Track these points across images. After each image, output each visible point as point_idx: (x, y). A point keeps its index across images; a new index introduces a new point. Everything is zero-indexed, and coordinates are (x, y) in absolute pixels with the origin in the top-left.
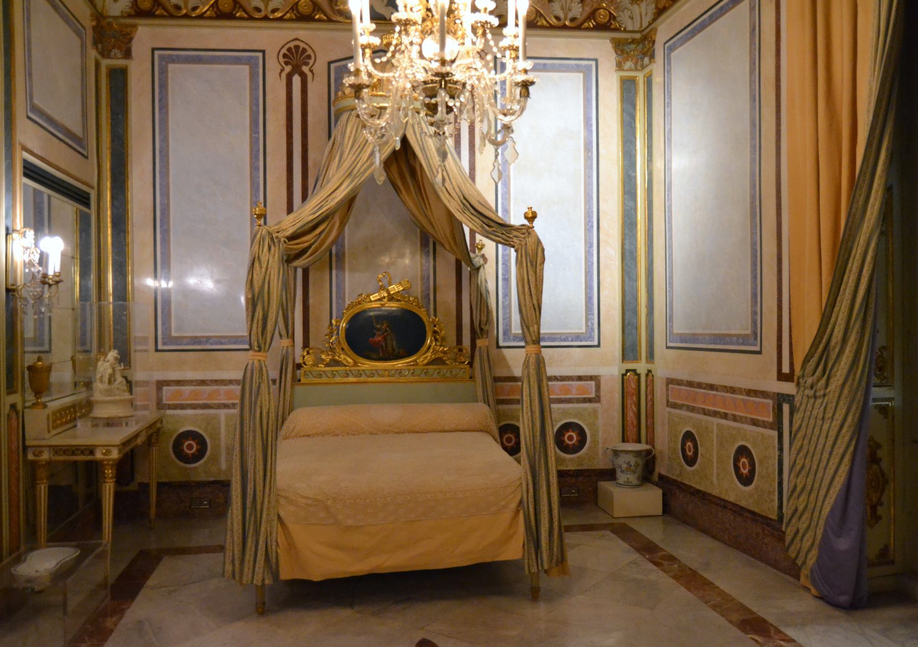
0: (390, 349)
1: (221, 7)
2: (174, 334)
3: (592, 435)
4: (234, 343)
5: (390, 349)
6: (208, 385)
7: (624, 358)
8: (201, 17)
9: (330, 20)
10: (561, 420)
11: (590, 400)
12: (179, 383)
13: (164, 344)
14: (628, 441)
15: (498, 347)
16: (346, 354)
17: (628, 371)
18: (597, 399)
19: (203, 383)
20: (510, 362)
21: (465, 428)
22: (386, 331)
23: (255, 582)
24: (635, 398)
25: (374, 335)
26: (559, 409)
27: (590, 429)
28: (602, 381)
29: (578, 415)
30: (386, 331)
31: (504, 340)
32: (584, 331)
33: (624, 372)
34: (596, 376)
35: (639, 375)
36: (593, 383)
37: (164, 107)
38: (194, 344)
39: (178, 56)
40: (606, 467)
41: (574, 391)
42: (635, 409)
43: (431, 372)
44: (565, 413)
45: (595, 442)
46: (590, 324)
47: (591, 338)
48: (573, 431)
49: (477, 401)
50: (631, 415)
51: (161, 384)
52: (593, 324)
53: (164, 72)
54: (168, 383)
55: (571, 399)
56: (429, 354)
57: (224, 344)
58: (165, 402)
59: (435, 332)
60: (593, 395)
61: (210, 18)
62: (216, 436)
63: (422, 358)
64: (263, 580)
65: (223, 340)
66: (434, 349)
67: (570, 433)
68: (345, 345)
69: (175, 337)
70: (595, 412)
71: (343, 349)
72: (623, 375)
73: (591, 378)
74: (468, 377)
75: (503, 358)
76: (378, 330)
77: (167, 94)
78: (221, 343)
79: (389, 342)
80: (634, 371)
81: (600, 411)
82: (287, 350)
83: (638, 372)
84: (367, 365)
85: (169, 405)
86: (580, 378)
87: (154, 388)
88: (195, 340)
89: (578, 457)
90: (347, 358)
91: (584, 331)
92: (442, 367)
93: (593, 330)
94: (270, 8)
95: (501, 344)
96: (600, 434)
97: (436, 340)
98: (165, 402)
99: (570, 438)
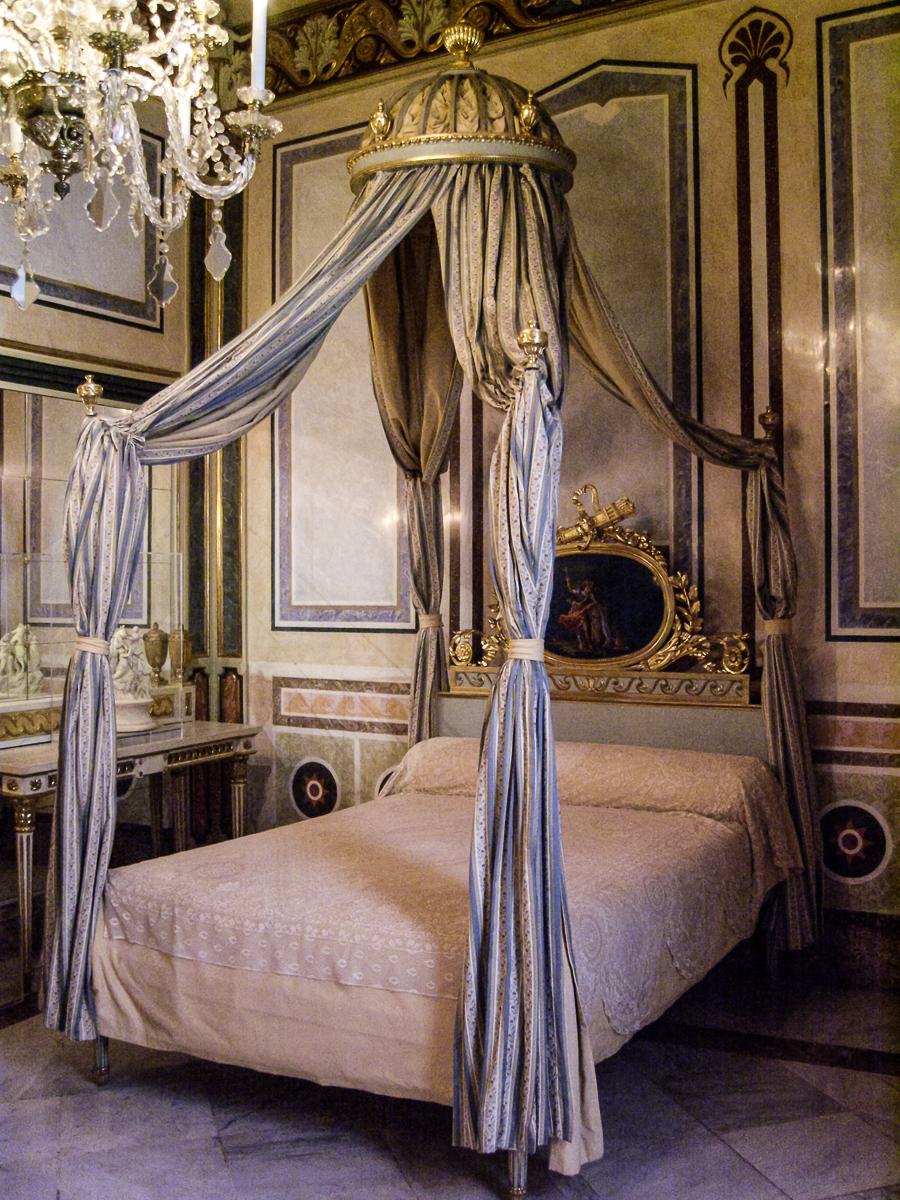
1: (360, 56)
2: (295, 603)
4: (373, 619)
6: (338, 689)
8: (335, 79)
9: (517, 30)
12: (300, 682)
13: (283, 618)
19: (331, 684)
22: (589, 601)
25: (568, 607)
37: (286, 235)
38: (320, 618)
39: (305, 150)
43: (674, 684)
51: (280, 683)
53: (287, 177)
54: (288, 682)
56: (671, 647)
57: (360, 620)
58: (284, 712)
59: (679, 603)
61: (348, 77)
62: (347, 775)
63: (662, 652)
65: (358, 614)
66: (680, 640)
69: (298, 607)
74: (746, 698)
76: (575, 597)
77: (290, 214)
78: (356, 619)
85: (289, 718)
87: (269, 687)
88: (320, 612)
92: (693, 675)
94: (426, 37)
97: (683, 620)
98: (284, 712)
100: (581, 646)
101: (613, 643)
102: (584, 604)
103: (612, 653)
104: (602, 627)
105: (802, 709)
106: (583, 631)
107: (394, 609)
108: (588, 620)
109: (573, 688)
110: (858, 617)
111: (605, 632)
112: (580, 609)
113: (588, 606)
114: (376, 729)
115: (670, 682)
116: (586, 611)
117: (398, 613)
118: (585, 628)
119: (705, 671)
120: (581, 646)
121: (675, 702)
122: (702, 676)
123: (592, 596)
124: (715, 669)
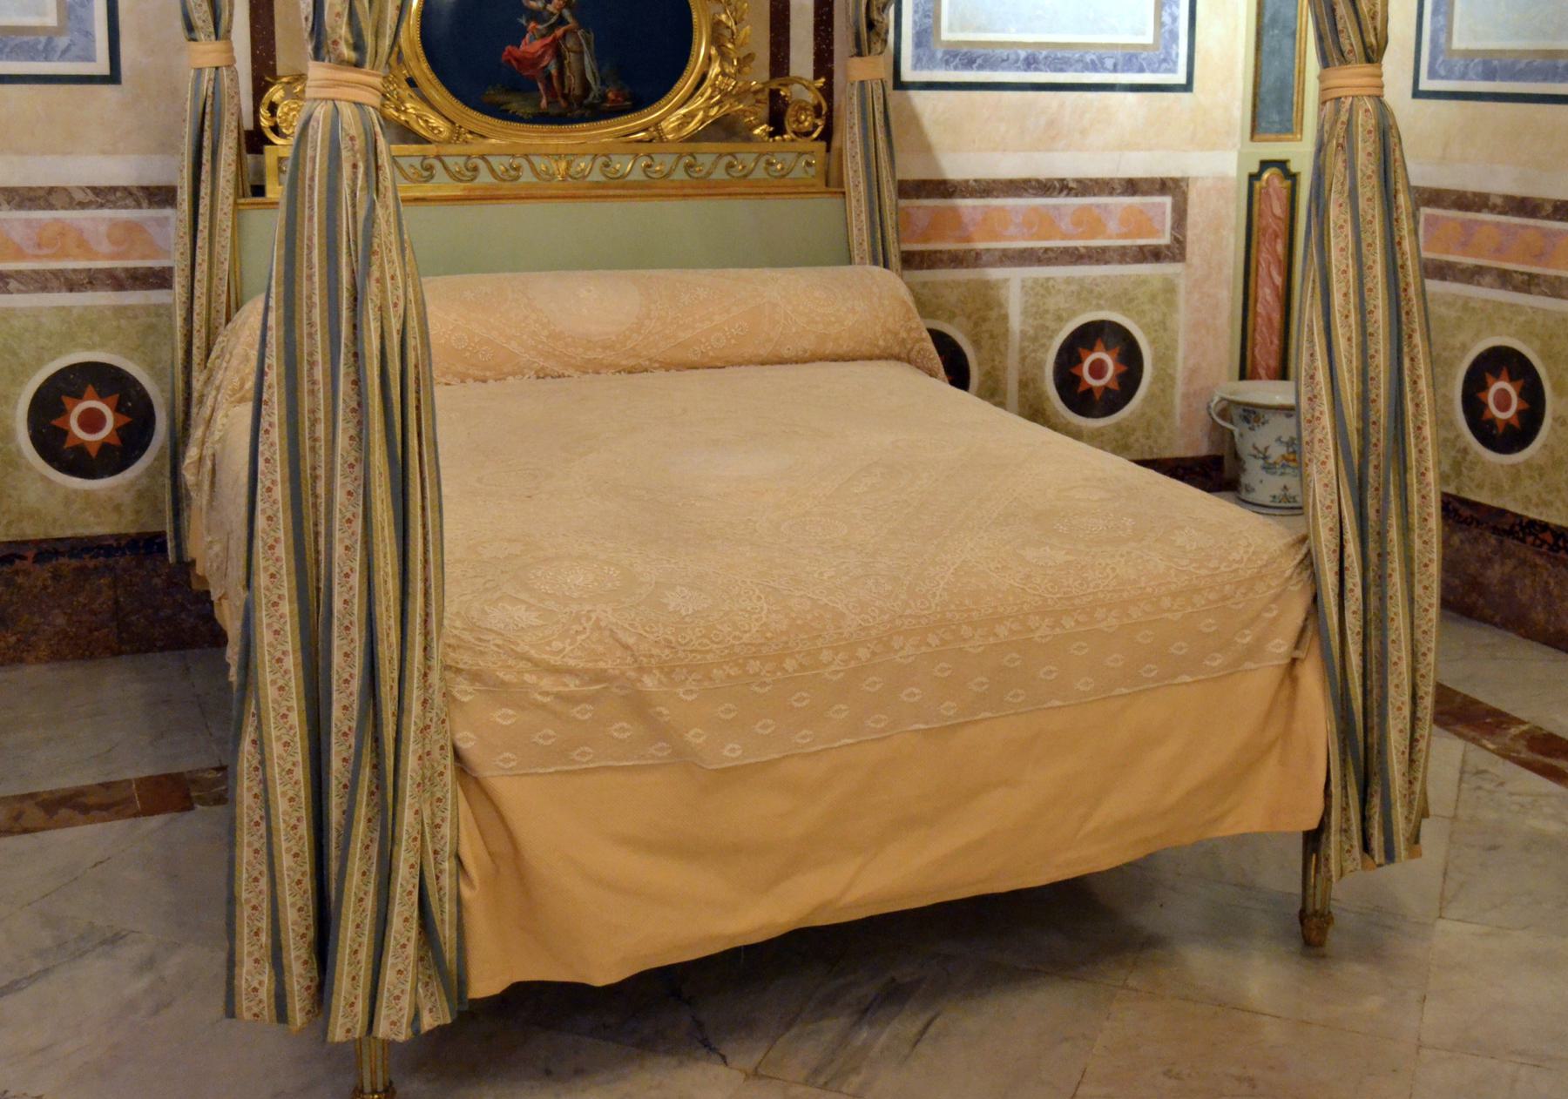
0: (573, 82)
3: (1159, 359)
5: (573, 82)
7: (1257, 127)
10: (1073, 313)
11: (1155, 255)
14: (1254, 376)
15: (900, 85)
16: (425, 100)
17: (1265, 165)
18: (1174, 252)
20: (934, 133)
21: (845, 347)
22: (561, 21)
23: (383, 1029)
24: (1280, 248)
26: (1069, 281)
27: (1152, 342)
28: (1193, 196)
29: (1123, 299)
30: (561, 21)
31: (917, 63)
32: (1148, 39)
33: (1255, 169)
34: (1176, 181)
35: (1293, 178)
36: (1167, 201)
40: (1190, 454)
41: (1113, 226)
42: (1278, 280)
43: (705, 161)
44: (1085, 293)
45: (1165, 378)
46: (1166, 18)
47: (1167, 62)
48: (1107, 349)
49: (850, 261)
50: (1267, 296)
52: (1175, 19)
55: (1104, 250)
60: (1165, 239)
63: (677, 113)
64: (416, 1017)
67: (1100, 355)
68: (421, 69)
70: (1170, 288)
71: (412, 83)
72: (1254, 178)
73: (1163, 186)
75: (914, 120)
76: (536, 16)
79: (571, 58)
80: (1282, 165)
81: (1182, 285)
82: (216, 80)
83: (1293, 168)
84: (502, 140)
86: (1132, 187)
89: (1118, 427)
90: (434, 113)
91: (1148, 39)
93: (1174, 36)
95: (908, 74)
96: (1180, 354)
99: (1098, 370)
100: (544, 102)
101: (604, 98)
102: (552, 28)
103: (598, 112)
104: (583, 65)
105: (889, 192)
106: (549, 77)
107: (50, 34)
108: (559, 57)
109: (527, 177)
110: (939, 55)
111: (589, 77)
112: (543, 36)
113: (559, 32)
114: (13, 284)
115: (700, 158)
116: (555, 40)
117: (62, 42)
118: (554, 71)
119: (758, 139)
120: (544, 102)
121: (705, 188)
122: (754, 147)
123: (566, 13)
124: (772, 135)
